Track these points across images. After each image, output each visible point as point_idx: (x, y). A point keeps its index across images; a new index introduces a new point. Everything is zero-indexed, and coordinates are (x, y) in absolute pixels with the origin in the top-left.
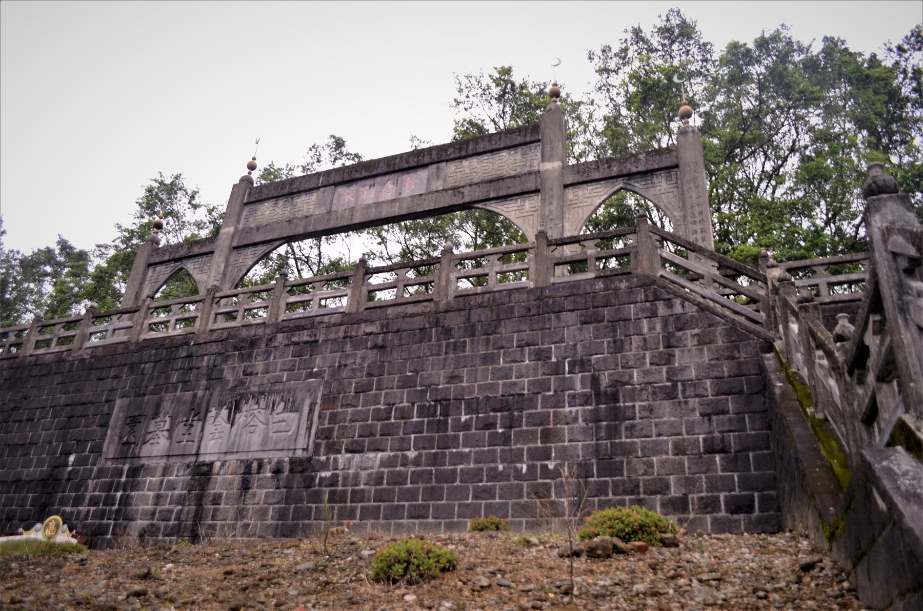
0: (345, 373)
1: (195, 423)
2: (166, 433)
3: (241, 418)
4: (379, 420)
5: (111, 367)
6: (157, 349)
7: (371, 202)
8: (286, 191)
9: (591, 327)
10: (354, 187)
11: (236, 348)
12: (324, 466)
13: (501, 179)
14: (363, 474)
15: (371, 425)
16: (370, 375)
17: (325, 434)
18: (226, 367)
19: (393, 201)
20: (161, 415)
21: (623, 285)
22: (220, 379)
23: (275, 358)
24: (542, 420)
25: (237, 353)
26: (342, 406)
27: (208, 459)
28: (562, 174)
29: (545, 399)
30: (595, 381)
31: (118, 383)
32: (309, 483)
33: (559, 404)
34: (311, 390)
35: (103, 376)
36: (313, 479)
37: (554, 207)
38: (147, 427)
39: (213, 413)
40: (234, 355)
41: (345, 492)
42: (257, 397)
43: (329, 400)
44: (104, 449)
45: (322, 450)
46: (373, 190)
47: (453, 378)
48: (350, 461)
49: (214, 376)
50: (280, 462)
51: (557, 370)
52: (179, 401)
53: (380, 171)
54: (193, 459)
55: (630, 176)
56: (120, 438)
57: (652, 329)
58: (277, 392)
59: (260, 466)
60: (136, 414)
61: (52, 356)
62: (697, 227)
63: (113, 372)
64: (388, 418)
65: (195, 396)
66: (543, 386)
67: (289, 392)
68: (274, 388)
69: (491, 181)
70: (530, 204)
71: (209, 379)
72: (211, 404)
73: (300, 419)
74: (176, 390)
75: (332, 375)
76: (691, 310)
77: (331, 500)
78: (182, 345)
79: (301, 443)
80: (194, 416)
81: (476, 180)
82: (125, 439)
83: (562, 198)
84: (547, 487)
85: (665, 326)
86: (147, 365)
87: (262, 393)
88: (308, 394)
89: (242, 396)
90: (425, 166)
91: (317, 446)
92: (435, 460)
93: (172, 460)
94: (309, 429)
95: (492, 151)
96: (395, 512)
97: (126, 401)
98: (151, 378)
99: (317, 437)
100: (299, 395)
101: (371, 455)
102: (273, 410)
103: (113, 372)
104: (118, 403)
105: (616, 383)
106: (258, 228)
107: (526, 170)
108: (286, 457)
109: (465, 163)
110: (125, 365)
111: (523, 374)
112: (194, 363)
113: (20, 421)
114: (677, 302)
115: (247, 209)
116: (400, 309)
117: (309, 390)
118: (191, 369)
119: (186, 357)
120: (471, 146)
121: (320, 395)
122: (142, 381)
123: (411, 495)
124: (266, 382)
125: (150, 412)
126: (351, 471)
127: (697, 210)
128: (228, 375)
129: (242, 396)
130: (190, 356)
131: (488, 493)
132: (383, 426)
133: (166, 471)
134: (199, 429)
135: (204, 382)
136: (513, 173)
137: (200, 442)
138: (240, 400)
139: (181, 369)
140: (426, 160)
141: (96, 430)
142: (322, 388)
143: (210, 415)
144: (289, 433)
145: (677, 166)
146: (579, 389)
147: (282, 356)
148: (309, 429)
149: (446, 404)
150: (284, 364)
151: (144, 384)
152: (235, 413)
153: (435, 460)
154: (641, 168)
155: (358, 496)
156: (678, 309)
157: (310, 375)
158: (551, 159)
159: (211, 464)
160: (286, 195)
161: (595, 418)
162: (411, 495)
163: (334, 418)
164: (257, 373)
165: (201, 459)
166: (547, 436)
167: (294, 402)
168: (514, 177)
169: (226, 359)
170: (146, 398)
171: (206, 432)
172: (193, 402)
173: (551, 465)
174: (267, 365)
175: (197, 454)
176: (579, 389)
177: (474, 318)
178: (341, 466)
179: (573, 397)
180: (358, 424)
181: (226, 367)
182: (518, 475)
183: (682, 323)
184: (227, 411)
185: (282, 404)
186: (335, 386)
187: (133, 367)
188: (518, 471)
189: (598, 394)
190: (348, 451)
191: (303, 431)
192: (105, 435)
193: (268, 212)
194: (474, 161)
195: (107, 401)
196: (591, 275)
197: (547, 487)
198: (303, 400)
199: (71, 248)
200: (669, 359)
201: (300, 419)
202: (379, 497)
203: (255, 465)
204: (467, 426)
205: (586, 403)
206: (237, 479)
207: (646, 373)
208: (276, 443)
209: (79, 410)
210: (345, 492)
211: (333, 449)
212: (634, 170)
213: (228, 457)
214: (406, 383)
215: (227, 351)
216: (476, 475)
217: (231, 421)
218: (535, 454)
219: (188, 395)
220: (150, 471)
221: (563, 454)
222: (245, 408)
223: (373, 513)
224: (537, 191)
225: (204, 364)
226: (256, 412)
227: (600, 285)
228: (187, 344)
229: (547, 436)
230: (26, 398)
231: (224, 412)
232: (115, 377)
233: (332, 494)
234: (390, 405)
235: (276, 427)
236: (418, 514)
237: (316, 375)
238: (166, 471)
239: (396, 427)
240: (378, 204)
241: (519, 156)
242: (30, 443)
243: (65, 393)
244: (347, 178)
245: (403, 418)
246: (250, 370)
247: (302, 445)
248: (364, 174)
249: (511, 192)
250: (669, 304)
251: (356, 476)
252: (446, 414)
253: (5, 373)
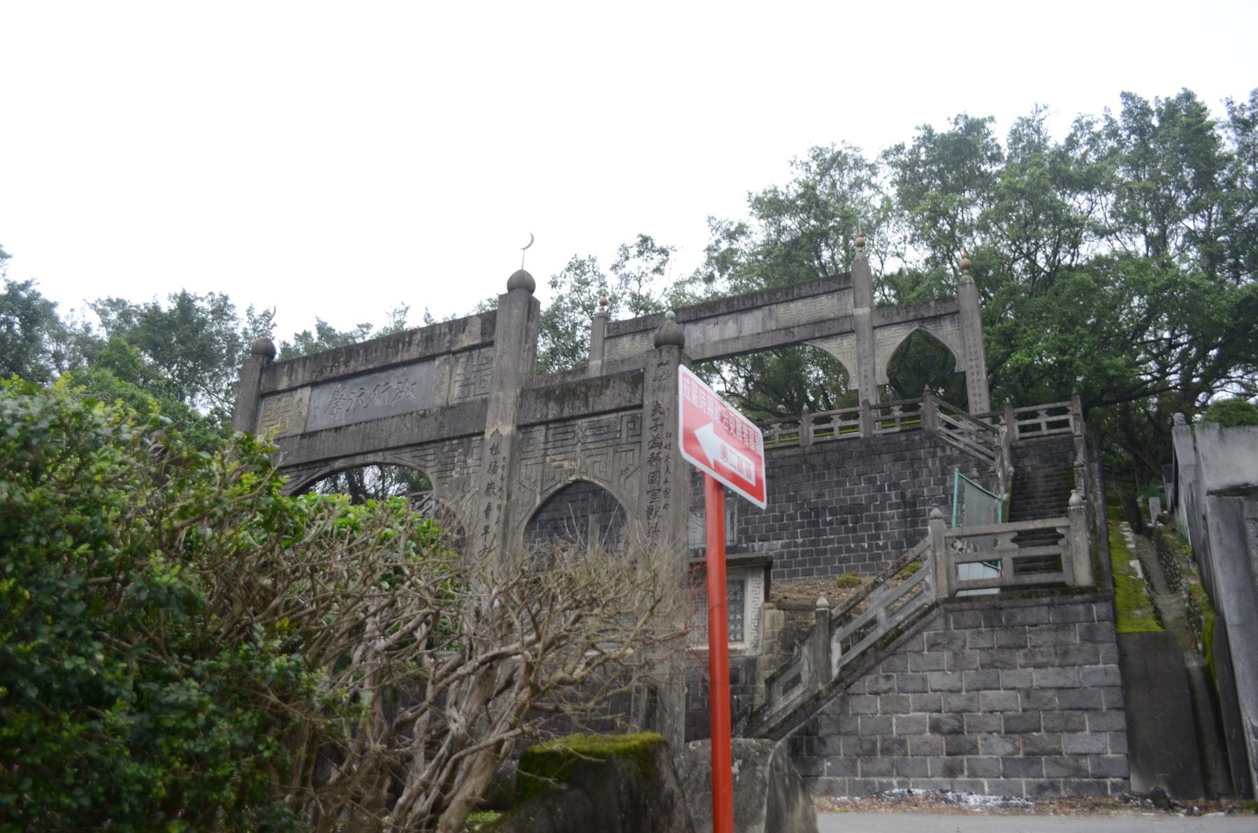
7: (717, 338)
8: (641, 328)
9: (899, 464)
10: (700, 325)
13: (823, 321)
17: (743, 531)
19: (737, 338)
21: (917, 438)
24: (875, 518)
28: (871, 319)
29: (875, 506)
30: (903, 495)
33: (883, 509)
37: (866, 346)
46: (717, 328)
47: (820, 495)
51: (881, 489)
53: (721, 311)
55: (923, 320)
57: (934, 464)
62: (973, 364)
63: (580, 497)
66: (874, 499)
69: (815, 323)
70: (848, 342)
76: (956, 453)
81: (803, 321)
83: (873, 338)
84: (879, 556)
85: (941, 463)
90: (759, 307)
92: (814, 543)
95: (813, 296)
96: (793, 574)
97: (597, 516)
103: (580, 497)
105: (915, 496)
106: (623, 361)
107: (842, 313)
109: (792, 305)
111: (861, 492)
114: (948, 448)
115: (608, 343)
116: (780, 453)
120: (796, 291)
123: (802, 563)
127: (973, 349)
131: (847, 560)
136: (832, 316)
140: (760, 303)
145: (958, 312)
146: (894, 500)
149: (818, 511)
153: (814, 543)
154: (931, 314)
156: (948, 452)
158: (861, 306)
160: (641, 332)
161: (903, 516)
162: (802, 563)
163: (747, 522)
166: (878, 527)
168: (832, 319)
173: (881, 543)
176: (894, 500)
177: (829, 458)
179: (891, 505)
182: (863, 549)
183: (951, 461)
188: (863, 548)
189: (905, 503)
193: (627, 346)
194: (800, 303)
196: (897, 429)
197: (879, 556)
199: (330, 329)
200: (943, 482)
202: (783, 566)
204: (831, 523)
205: (899, 508)
207: (931, 490)
211: (750, 539)
212: (926, 315)
214: (791, 499)
216: (839, 550)
218: (871, 538)
221: (887, 536)
224: (852, 332)
227: (903, 438)
229: (878, 527)
232: (583, 500)
234: (782, 512)
236: (808, 573)
239: (788, 525)
240: (724, 341)
241: (835, 300)
244: (693, 317)
248: (708, 314)
249: (832, 332)
250: (944, 449)
252: (817, 517)
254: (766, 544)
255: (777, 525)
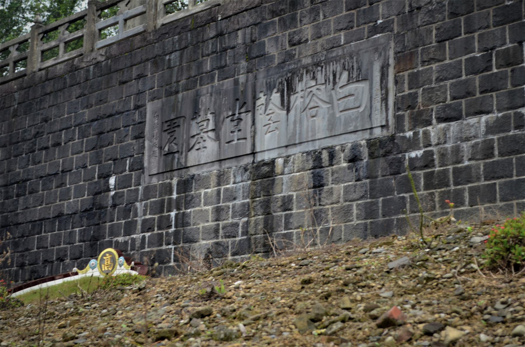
0: (420, 18)
1: (243, 116)
2: (211, 134)
3: (297, 100)
4: (476, 73)
5: (132, 66)
6: (179, 33)
11: (274, 13)
12: (413, 144)
14: (465, 146)
15: (466, 81)
16: (454, 14)
17: (406, 103)
18: (266, 39)
20: (202, 113)
22: (262, 55)
23: (325, 17)
25: (277, 19)
26: (423, 62)
27: (267, 157)
31: (144, 84)
32: (396, 168)
34: (379, 49)
35: (124, 79)
36: (400, 161)
38: (189, 130)
39: (262, 99)
40: (273, 23)
41: (445, 173)
42: (311, 70)
43: (404, 58)
44: (146, 164)
45: (407, 124)
48: (445, 131)
49: (254, 54)
50: (355, 147)
52: (219, 92)
54: (248, 160)
56: (161, 148)
58: (336, 60)
59: (332, 156)
60: (173, 117)
61: (62, 66)
63: (135, 72)
64: (489, 68)
65: (236, 82)
67: (351, 58)
68: (330, 56)
71: (249, 58)
72: (258, 90)
73: (371, 89)
74: (213, 80)
75: (403, 24)
77: (427, 187)
78: (208, 22)
79: (378, 119)
80: (240, 109)
82: (166, 149)
86: (173, 56)
87: (317, 64)
88: (376, 56)
89: (293, 72)
91: (399, 119)
93: (226, 165)
94: (385, 99)
97: (158, 103)
98: (181, 69)
99: (397, 108)
100: (365, 59)
101: (473, 120)
102: (335, 83)
103: (135, 72)
104: (150, 107)
108: (361, 139)
110: (147, 60)
112: (228, 42)
113: (46, 148)
117: (376, 50)
118: (225, 50)
119: (217, 36)
121: (391, 53)
122: (171, 76)
124: (319, 49)
125: (187, 111)
126: (449, 146)
128: (271, 49)
129: (293, 72)
130: (220, 35)
132: (483, 80)
133: (221, 179)
134: (250, 122)
135: (243, 64)
137: (254, 137)
138: (292, 78)
139: (213, 53)
141: (131, 144)
142: (392, 44)
143: (258, 103)
144: (361, 109)
147: (334, 13)
148: (385, 99)
150: (338, 21)
151: (174, 79)
152: (289, 96)
155: (463, 176)
157: (375, 30)
159: (272, 163)
164: (307, 40)
165: (259, 158)
167: (359, 69)
169: (264, 30)
170: (180, 95)
171: (259, 125)
172: (236, 90)
174: (317, 27)
175: (253, 153)
178: (434, 140)
180: (448, 83)
181: (266, 39)
184: (278, 95)
185: (345, 75)
186: (409, 37)
187: (157, 61)
190: (440, 120)
191: (377, 104)
192: (143, 147)
195: (137, 107)
198: (371, 64)
201: (371, 89)
203: (325, 155)
206: (307, 176)
208: (347, 123)
209: (108, 124)
210: (445, 173)
211: (421, 120)
213: (292, 151)
215: (264, 19)
217: (286, 106)
219: (228, 83)
220: (204, 182)
222: (299, 87)
223: (489, 195)
225: (240, 40)
226: (314, 89)
228: (214, 19)
230: (46, 121)
231: (276, 97)
232: (140, 77)
233: (429, 177)
234: (488, 50)
235: (342, 104)
237: (382, 29)
238: (221, 179)
239: (502, 77)
242: (63, 171)
243: (87, 107)
245: (508, 65)
246: (297, 38)
247: (381, 122)
251: (457, 150)
253: (16, 95)
254: (454, 126)
255: (477, 79)
